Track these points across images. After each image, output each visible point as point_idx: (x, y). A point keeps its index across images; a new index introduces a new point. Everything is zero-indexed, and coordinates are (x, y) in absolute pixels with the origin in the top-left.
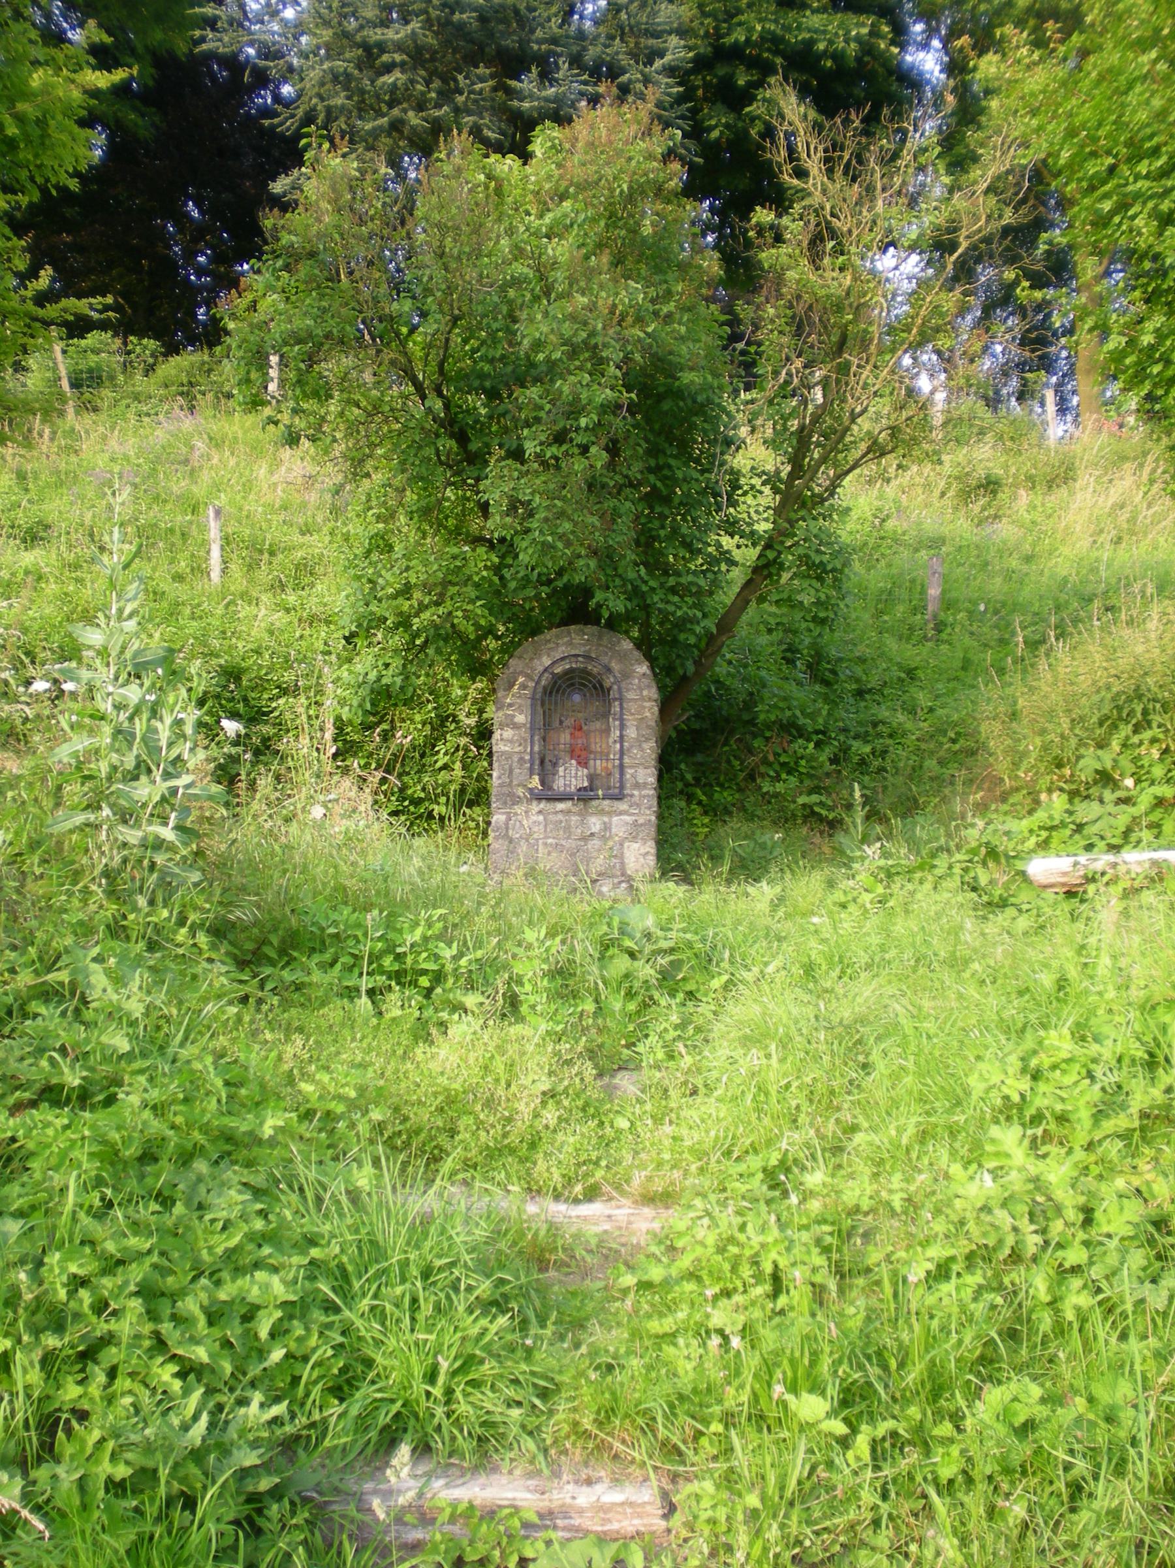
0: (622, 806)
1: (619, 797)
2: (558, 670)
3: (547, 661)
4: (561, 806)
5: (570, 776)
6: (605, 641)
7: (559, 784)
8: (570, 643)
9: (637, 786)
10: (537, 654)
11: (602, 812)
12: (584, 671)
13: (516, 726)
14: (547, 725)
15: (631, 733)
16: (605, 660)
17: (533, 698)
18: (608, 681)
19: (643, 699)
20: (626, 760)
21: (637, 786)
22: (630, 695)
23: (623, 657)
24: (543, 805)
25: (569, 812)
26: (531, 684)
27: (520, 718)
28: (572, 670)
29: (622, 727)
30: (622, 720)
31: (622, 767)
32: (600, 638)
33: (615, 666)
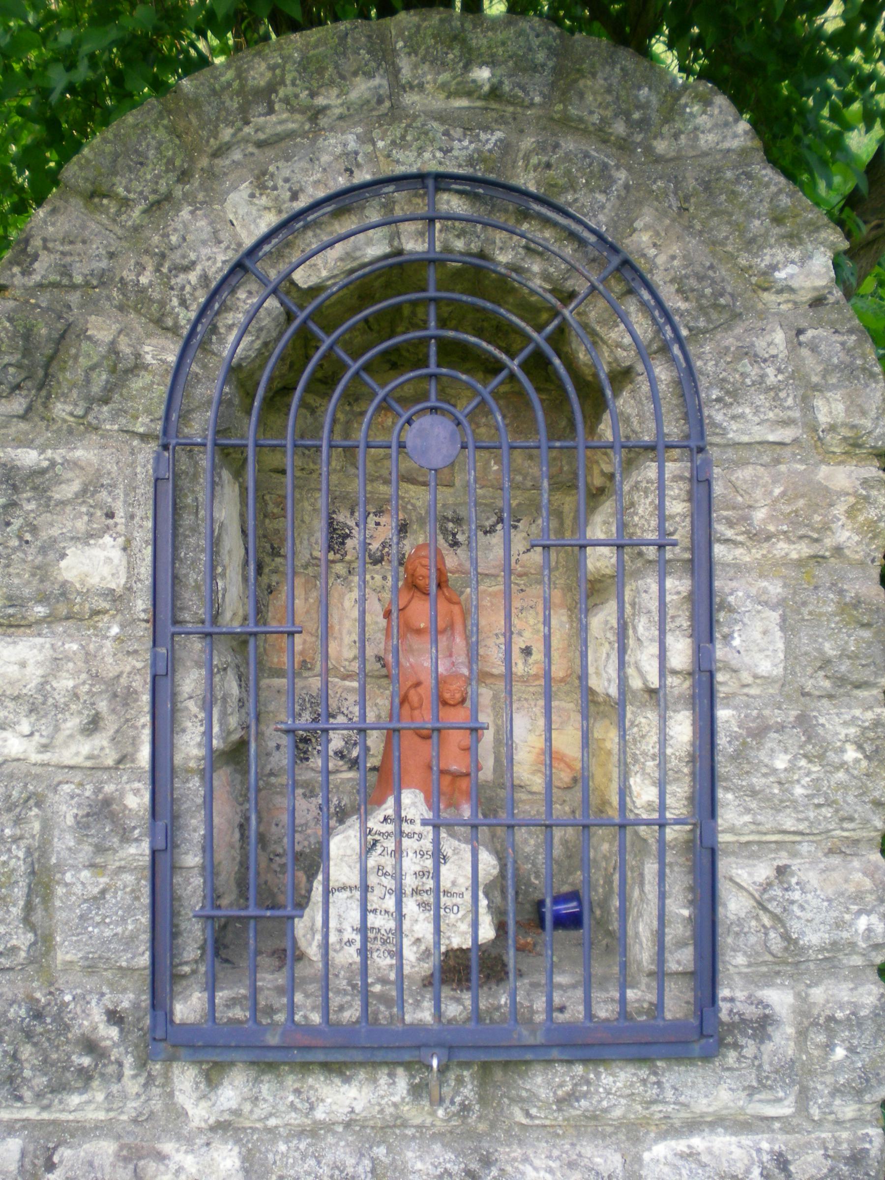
0: (709, 1090)
1: (700, 1033)
2: (321, 267)
3: (250, 217)
4: (343, 1098)
5: (395, 891)
6: (592, 101)
7: (332, 924)
8: (388, 112)
9: (791, 960)
10: (194, 173)
11: (593, 1124)
12: (476, 274)
13: (66, 608)
14: (266, 554)
15: (755, 648)
16: (599, 210)
17: (169, 439)
18: (618, 335)
19: (817, 443)
20: (732, 814)
21: (791, 960)
22: (744, 423)
23: (699, 197)
24: (231, 1093)
25: (387, 1129)
26: (160, 352)
27: (102, 563)
28: (397, 271)
29: (707, 617)
30: (702, 567)
31: (705, 860)
32: (565, 78)
33: (657, 246)
